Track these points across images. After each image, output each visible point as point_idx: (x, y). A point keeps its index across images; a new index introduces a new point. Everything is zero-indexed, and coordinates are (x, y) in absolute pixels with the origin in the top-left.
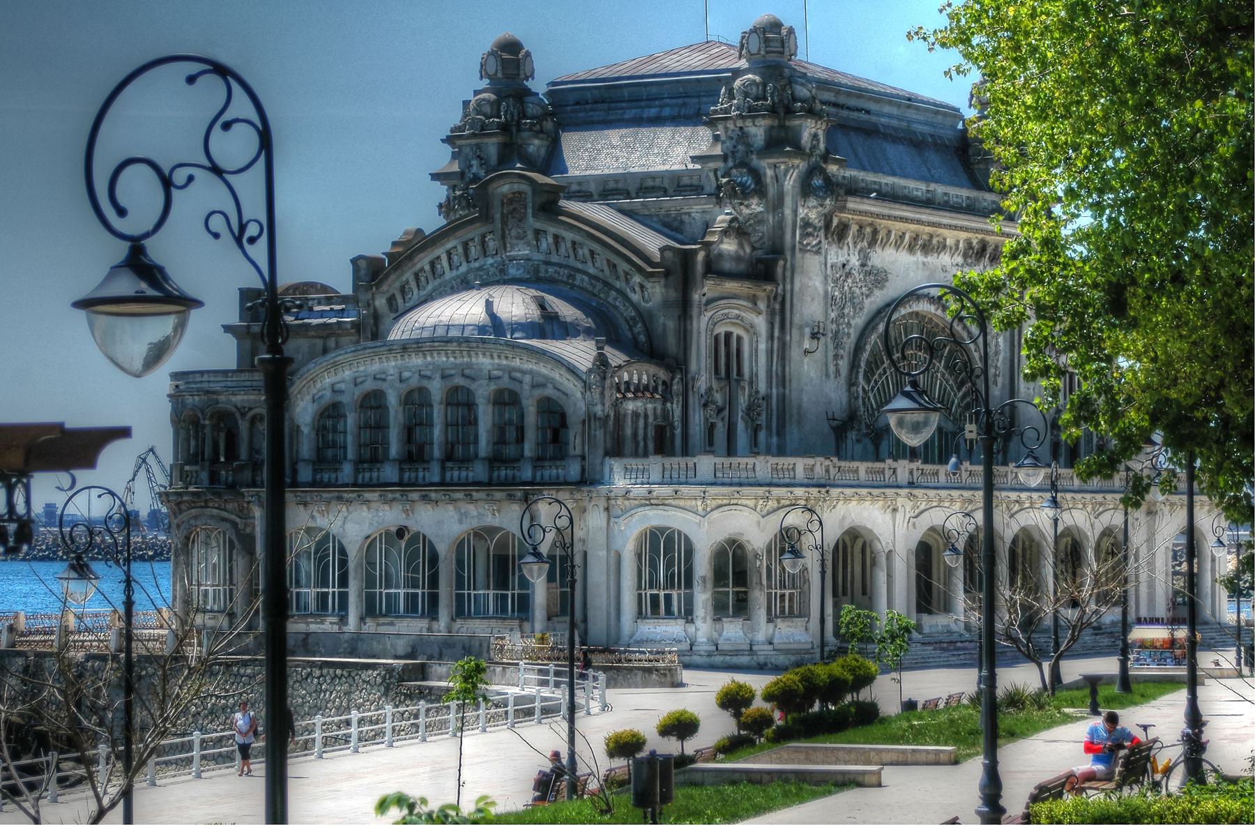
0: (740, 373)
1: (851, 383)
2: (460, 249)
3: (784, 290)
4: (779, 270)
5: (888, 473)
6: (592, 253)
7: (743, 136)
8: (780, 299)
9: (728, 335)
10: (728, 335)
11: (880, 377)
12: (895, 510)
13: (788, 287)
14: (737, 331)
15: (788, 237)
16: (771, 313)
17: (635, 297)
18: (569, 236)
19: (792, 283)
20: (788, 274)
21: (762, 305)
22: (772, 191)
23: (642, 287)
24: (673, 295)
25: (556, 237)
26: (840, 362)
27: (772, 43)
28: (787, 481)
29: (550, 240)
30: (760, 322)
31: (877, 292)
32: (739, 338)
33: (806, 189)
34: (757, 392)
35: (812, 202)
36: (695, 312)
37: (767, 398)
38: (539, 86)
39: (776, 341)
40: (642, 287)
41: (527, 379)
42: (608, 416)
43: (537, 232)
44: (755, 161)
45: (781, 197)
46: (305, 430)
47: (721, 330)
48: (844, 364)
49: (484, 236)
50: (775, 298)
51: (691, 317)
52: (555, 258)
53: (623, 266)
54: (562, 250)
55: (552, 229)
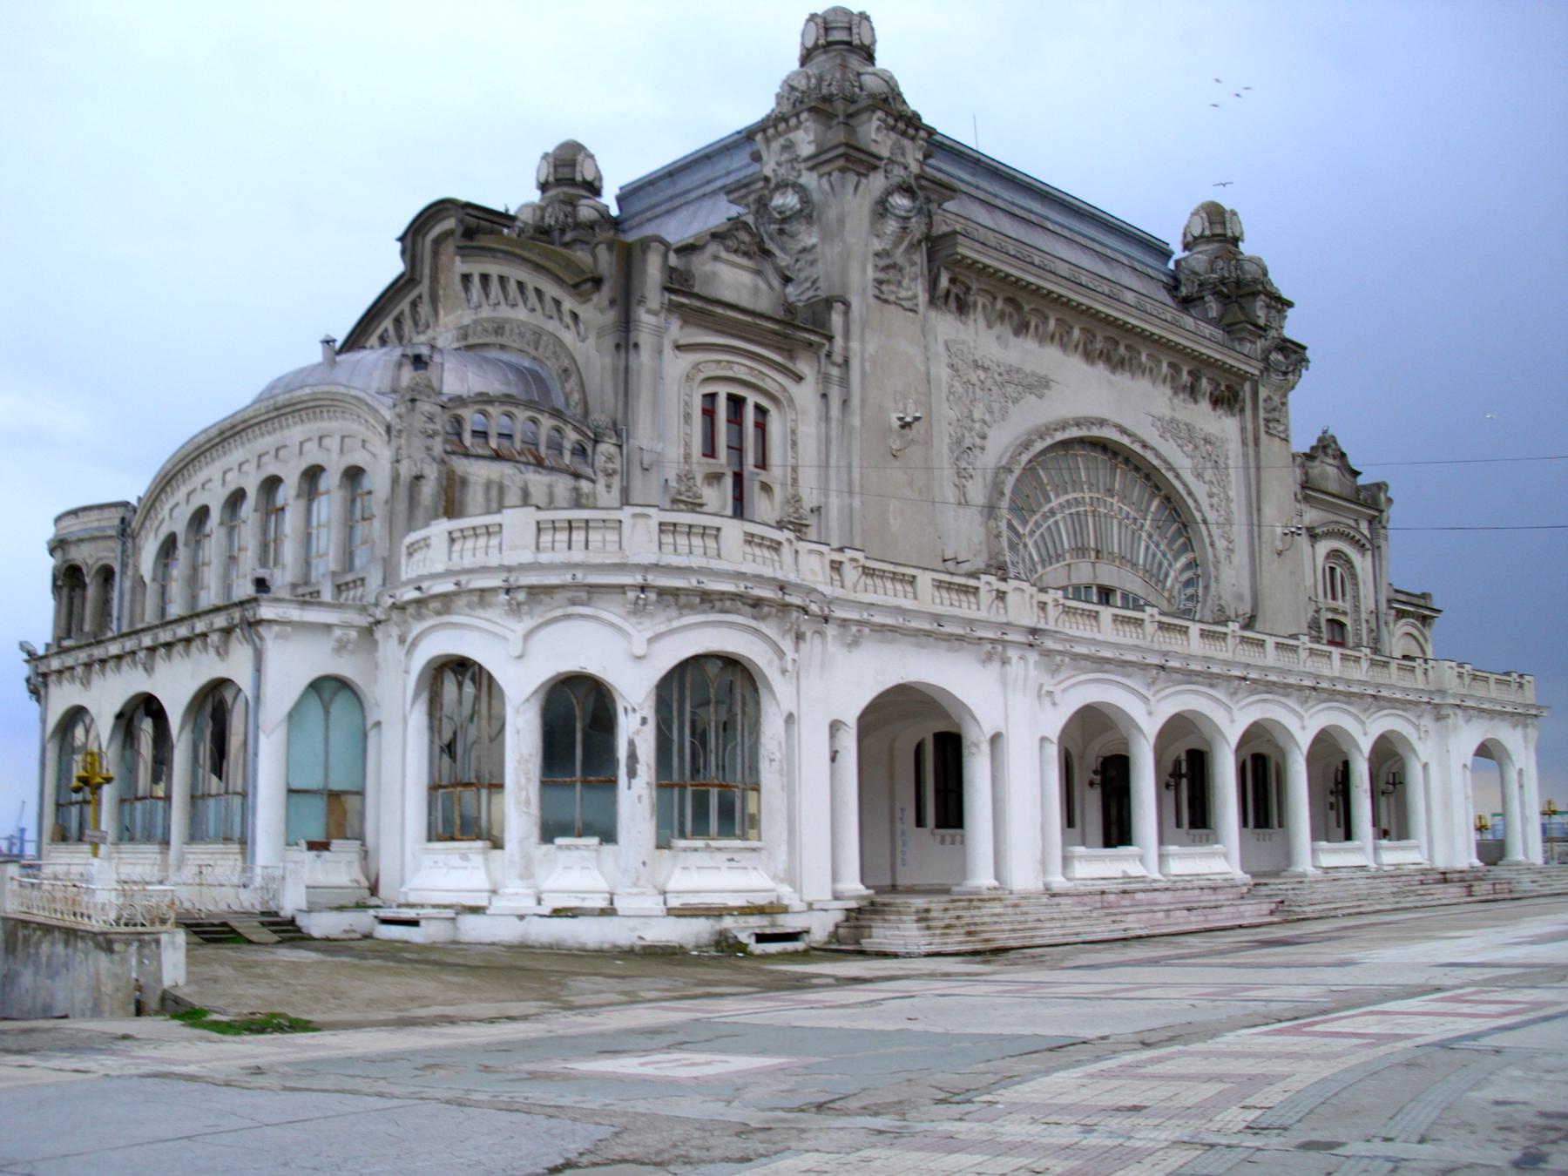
0: (762, 464)
1: (990, 511)
2: (391, 331)
3: (846, 349)
4: (836, 319)
5: (986, 597)
6: (520, 285)
7: (789, 146)
8: (838, 358)
9: (736, 402)
10: (736, 402)
11: (1045, 518)
12: (1005, 662)
13: (855, 345)
14: (752, 399)
15: (855, 277)
16: (826, 379)
17: (568, 337)
18: (494, 269)
19: (862, 341)
20: (855, 328)
21: (804, 366)
22: (832, 214)
23: (575, 316)
24: (611, 316)
25: (485, 278)
26: (969, 484)
27: (840, 43)
28: (697, 561)
29: (476, 280)
30: (805, 394)
31: (1031, 399)
32: (761, 411)
33: (882, 209)
34: (796, 499)
35: (892, 226)
36: (645, 338)
37: (817, 510)
38: (609, 200)
39: (834, 424)
40: (575, 316)
41: (333, 443)
42: (419, 478)
43: (466, 278)
44: (809, 179)
45: (841, 221)
46: (147, 579)
47: (723, 391)
48: (977, 492)
49: (414, 305)
50: (829, 355)
51: (636, 346)
52: (486, 312)
53: (551, 290)
54: (492, 296)
55: (476, 268)
